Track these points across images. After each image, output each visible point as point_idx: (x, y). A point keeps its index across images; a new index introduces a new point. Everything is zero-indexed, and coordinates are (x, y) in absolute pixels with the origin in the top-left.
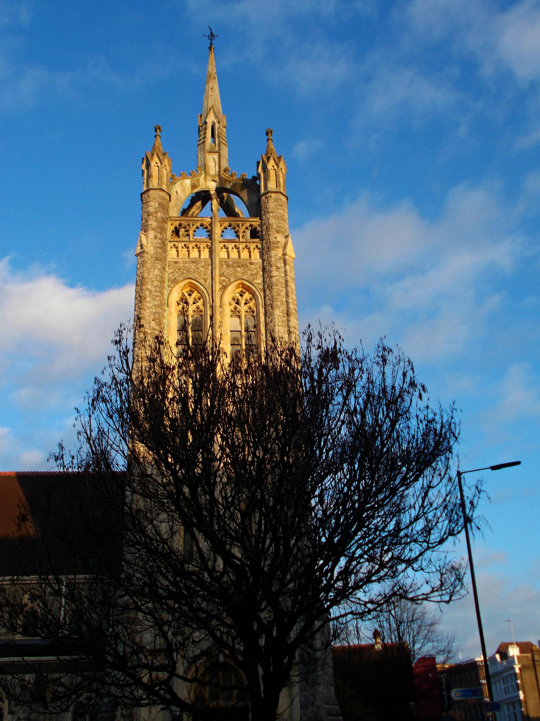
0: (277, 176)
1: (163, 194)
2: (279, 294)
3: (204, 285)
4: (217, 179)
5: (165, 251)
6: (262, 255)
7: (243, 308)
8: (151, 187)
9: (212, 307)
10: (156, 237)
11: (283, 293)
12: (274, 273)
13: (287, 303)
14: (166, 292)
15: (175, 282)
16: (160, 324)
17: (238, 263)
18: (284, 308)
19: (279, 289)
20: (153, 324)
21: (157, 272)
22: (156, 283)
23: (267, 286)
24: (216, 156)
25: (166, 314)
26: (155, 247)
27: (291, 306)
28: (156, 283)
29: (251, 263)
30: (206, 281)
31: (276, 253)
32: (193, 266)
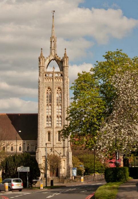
0: (66, 62)
1: (43, 67)
2: (66, 90)
3: (51, 87)
4: (54, 57)
5: (44, 81)
6: (63, 81)
7: (59, 92)
8: (41, 66)
9: (53, 93)
10: (42, 78)
11: (67, 90)
12: (65, 86)
13: (67, 92)
14: (44, 90)
15: (46, 87)
16: (43, 97)
17: (58, 83)
18: (67, 93)
19: (66, 89)
20: (42, 97)
21: (42, 86)
22: (42, 88)
23: (64, 88)
24: (54, 50)
25: (44, 95)
26: (42, 80)
27: (68, 93)
28: (42, 88)
29: (61, 83)
30: (52, 87)
31: (65, 81)
32: (49, 83)
